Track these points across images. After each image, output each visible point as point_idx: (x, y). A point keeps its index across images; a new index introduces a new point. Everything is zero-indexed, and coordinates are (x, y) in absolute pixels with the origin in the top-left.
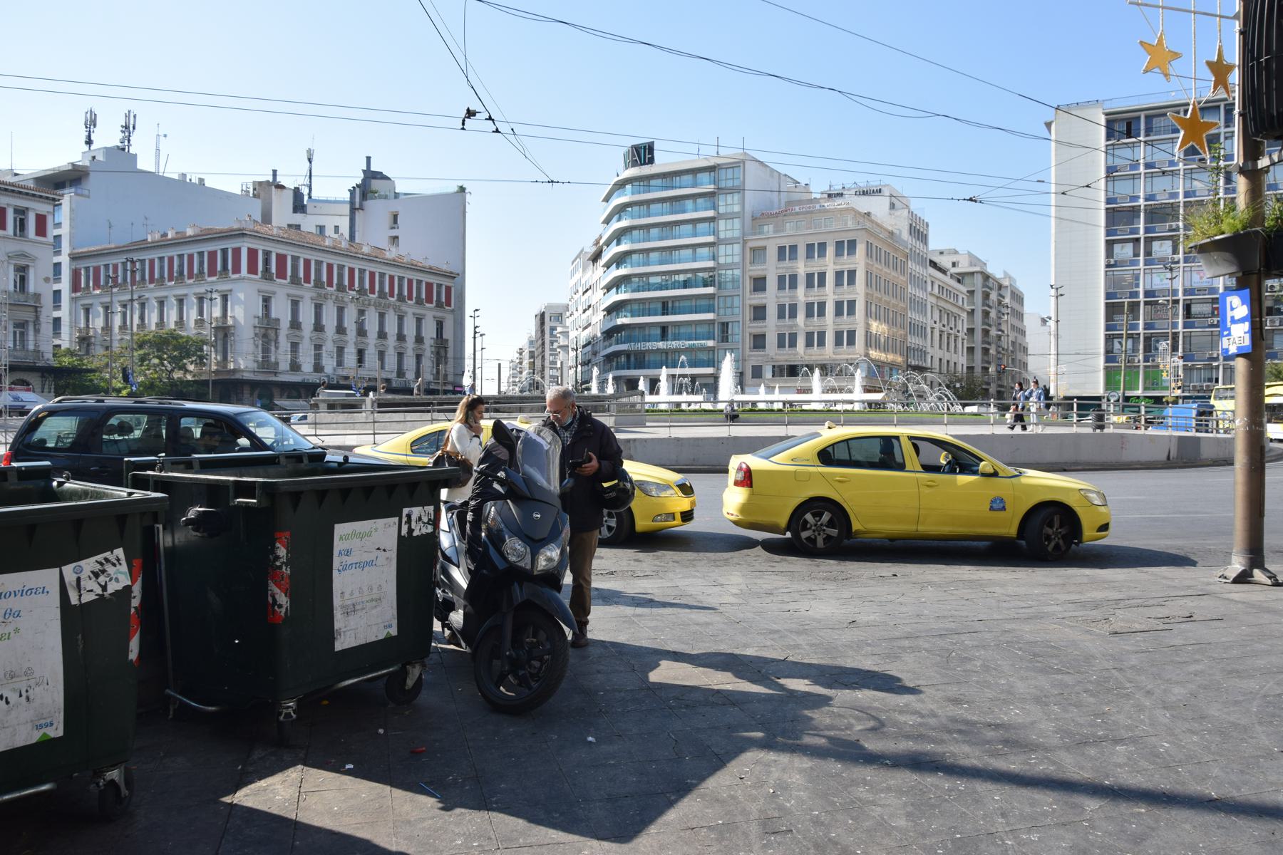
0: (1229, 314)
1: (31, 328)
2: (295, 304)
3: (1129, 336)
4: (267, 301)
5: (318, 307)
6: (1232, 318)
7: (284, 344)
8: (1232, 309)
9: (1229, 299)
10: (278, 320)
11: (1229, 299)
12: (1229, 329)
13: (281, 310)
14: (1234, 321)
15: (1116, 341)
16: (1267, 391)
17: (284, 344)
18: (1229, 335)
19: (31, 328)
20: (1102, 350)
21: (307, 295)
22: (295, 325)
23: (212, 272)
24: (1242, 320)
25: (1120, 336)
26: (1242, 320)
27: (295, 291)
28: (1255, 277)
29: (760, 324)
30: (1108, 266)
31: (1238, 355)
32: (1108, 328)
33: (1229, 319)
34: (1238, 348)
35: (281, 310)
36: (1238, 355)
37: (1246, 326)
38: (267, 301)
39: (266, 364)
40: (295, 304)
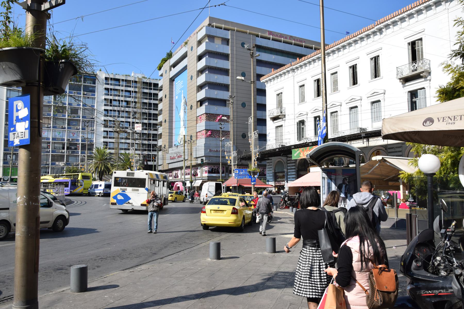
0: (15, 114)
3: (14, 154)
6: (17, 117)
8: (17, 110)
9: (15, 103)
11: (15, 103)
12: (15, 126)
14: (18, 120)
15: (8, 156)
16: (42, 178)
18: (15, 130)
20: (2, 158)
24: (23, 120)
25: (10, 154)
26: (23, 120)
28: (36, 88)
30: (6, 125)
31: (21, 147)
32: (5, 150)
33: (15, 118)
34: (20, 141)
36: (21, 147)
37: (26, 124)
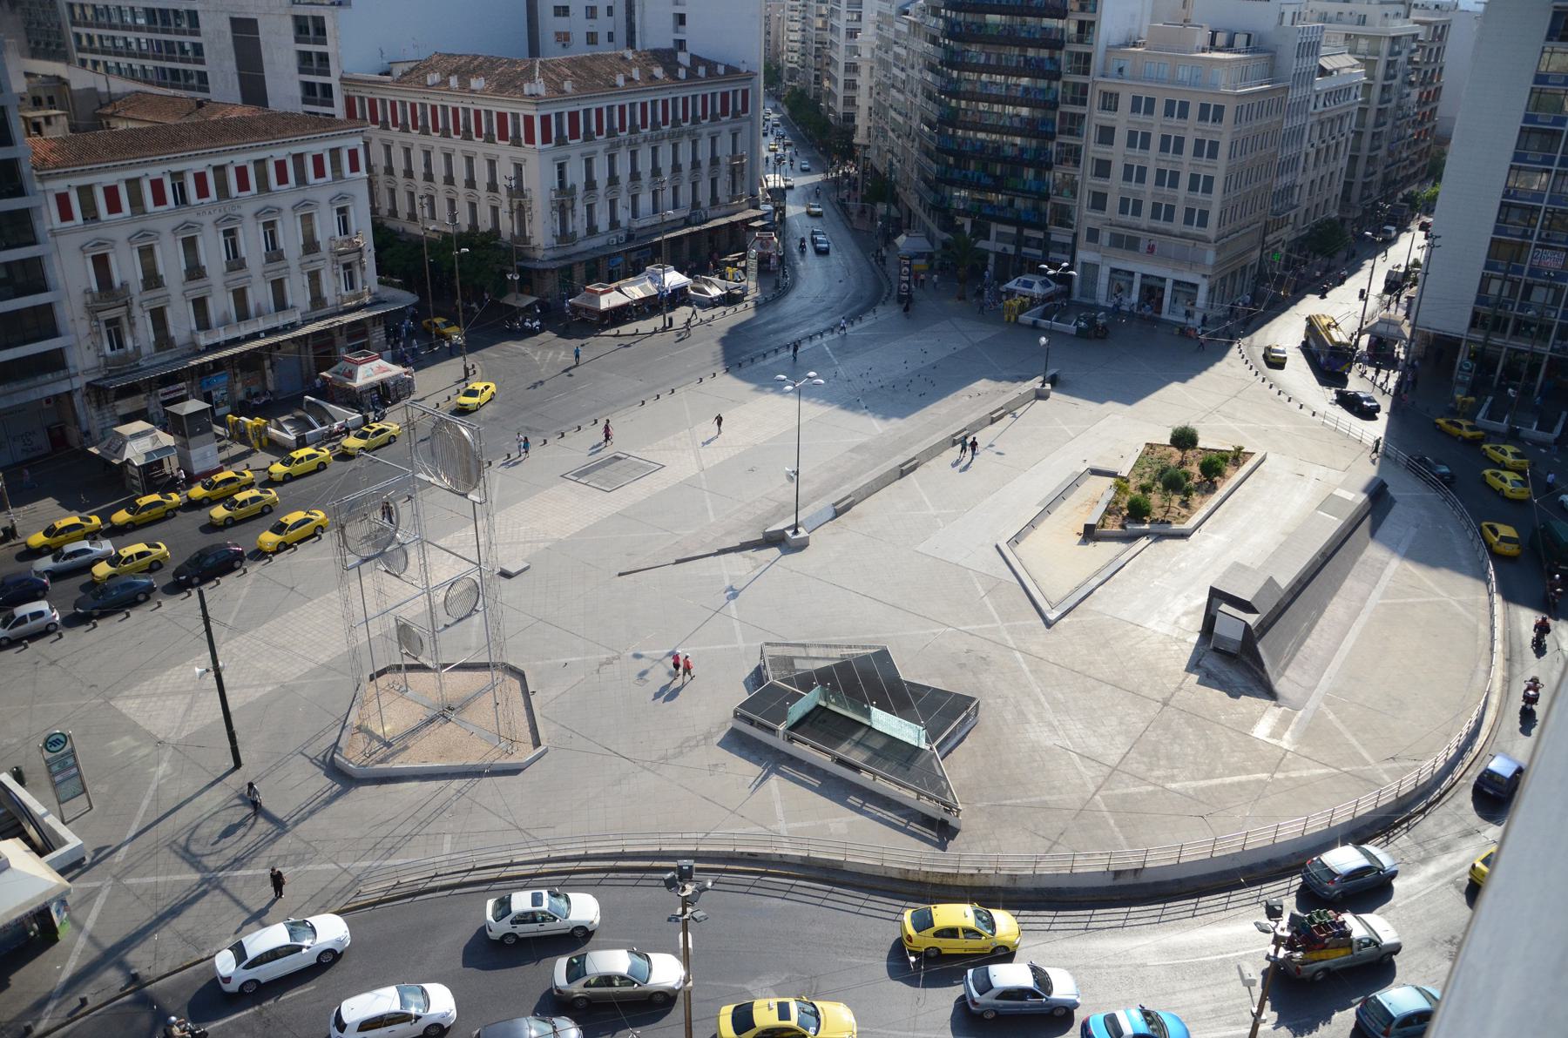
1: (358, 269)
2: (589, 162)
4: (561, 167)
5: (612, 158)
7: (581, 209)
10: (573, 187)
13: (576, 176)
17: (581, 209)
19: (358, 269)
21: (601, 145)
22: (590, 185)
23: (503, 136)
27: (588, 148)
29: (1102, 182)
35: (576, 176)
38: (561, 167)
39: (565, 236)
40: (589, 162)
